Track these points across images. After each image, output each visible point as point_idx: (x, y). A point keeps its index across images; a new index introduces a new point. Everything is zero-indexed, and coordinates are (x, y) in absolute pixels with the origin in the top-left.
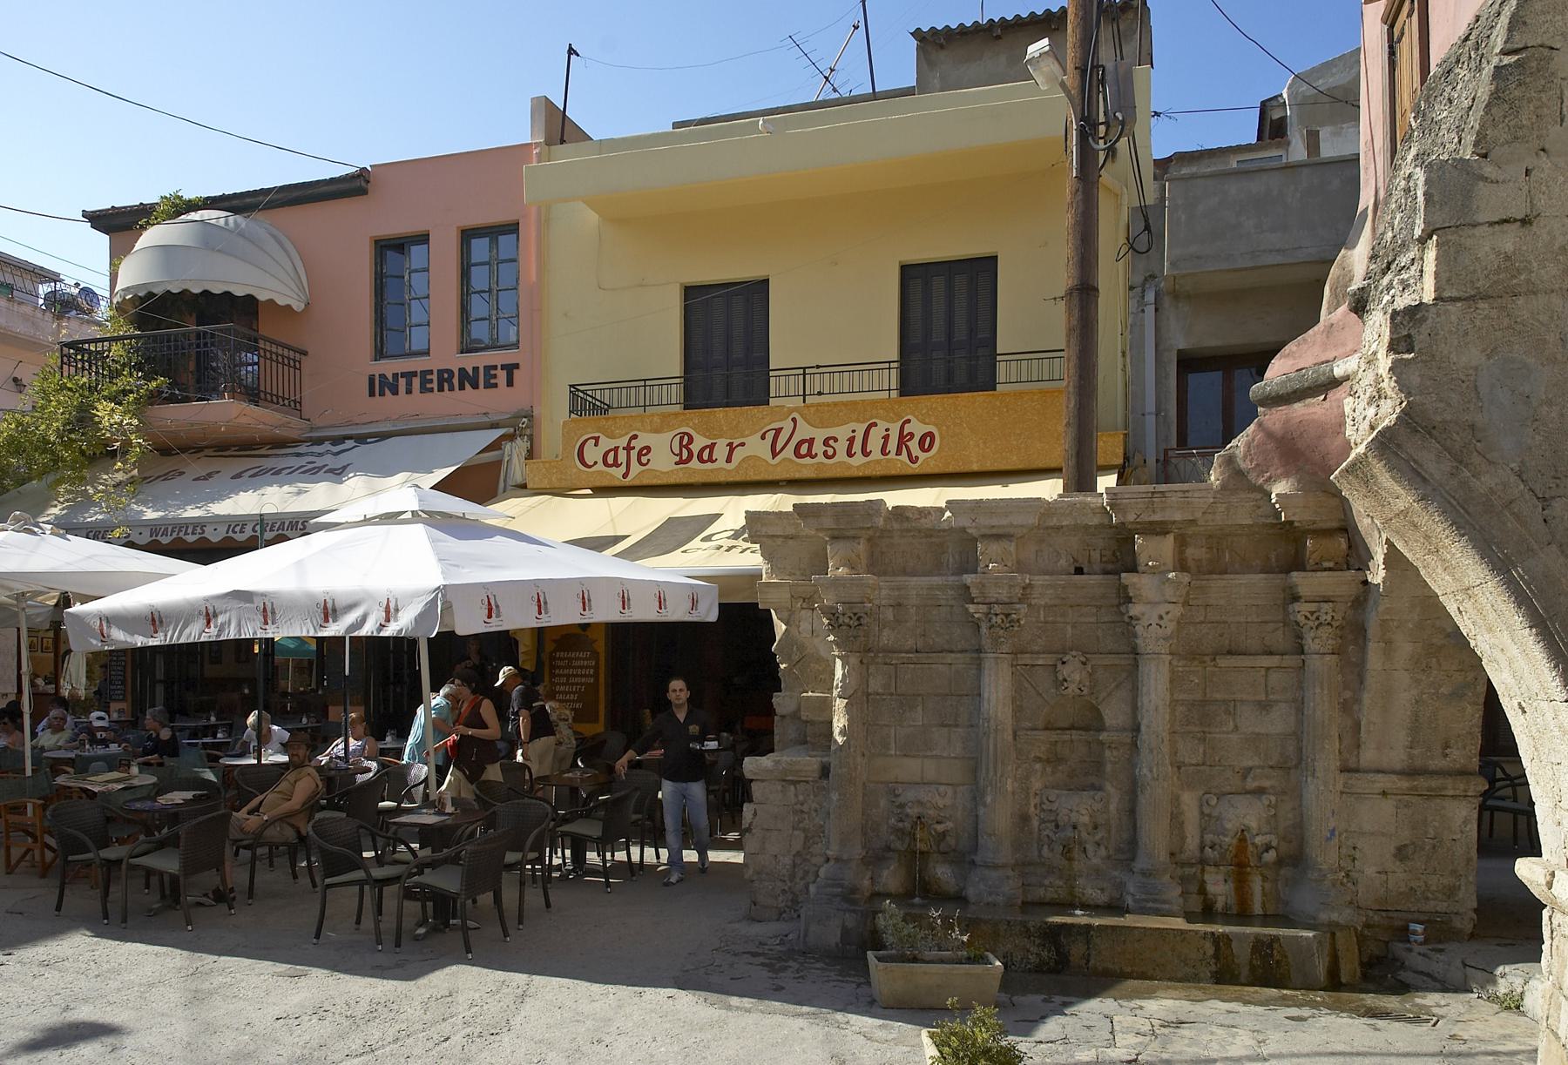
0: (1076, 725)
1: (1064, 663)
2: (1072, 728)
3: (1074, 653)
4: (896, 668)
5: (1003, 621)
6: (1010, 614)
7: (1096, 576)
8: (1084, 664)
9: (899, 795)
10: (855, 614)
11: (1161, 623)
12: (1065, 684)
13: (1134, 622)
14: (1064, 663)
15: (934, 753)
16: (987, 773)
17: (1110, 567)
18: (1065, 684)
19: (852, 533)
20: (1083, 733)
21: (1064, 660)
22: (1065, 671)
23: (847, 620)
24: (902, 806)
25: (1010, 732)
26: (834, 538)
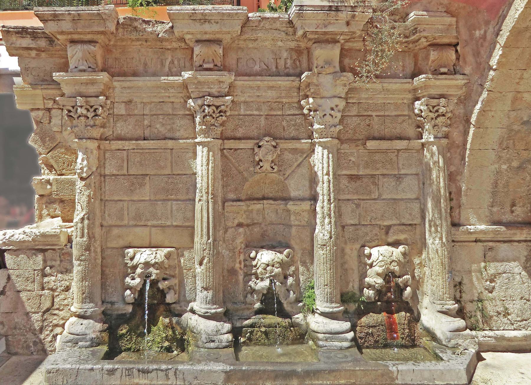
0: (266, 196)
1: (260, 147)
2: (264, 198)
3: (267, 139)
4: (128, 153)
5: (214, 112)
6: (220, 106)
8: (275, 147)
12: (261, 164)
14: (260, 147)
15: (160, 222)
19: (89, 37)
21: (260, 144)
22: (260, 154)
23: (84, 112)
25: (220, 203)
26: (73, 42)
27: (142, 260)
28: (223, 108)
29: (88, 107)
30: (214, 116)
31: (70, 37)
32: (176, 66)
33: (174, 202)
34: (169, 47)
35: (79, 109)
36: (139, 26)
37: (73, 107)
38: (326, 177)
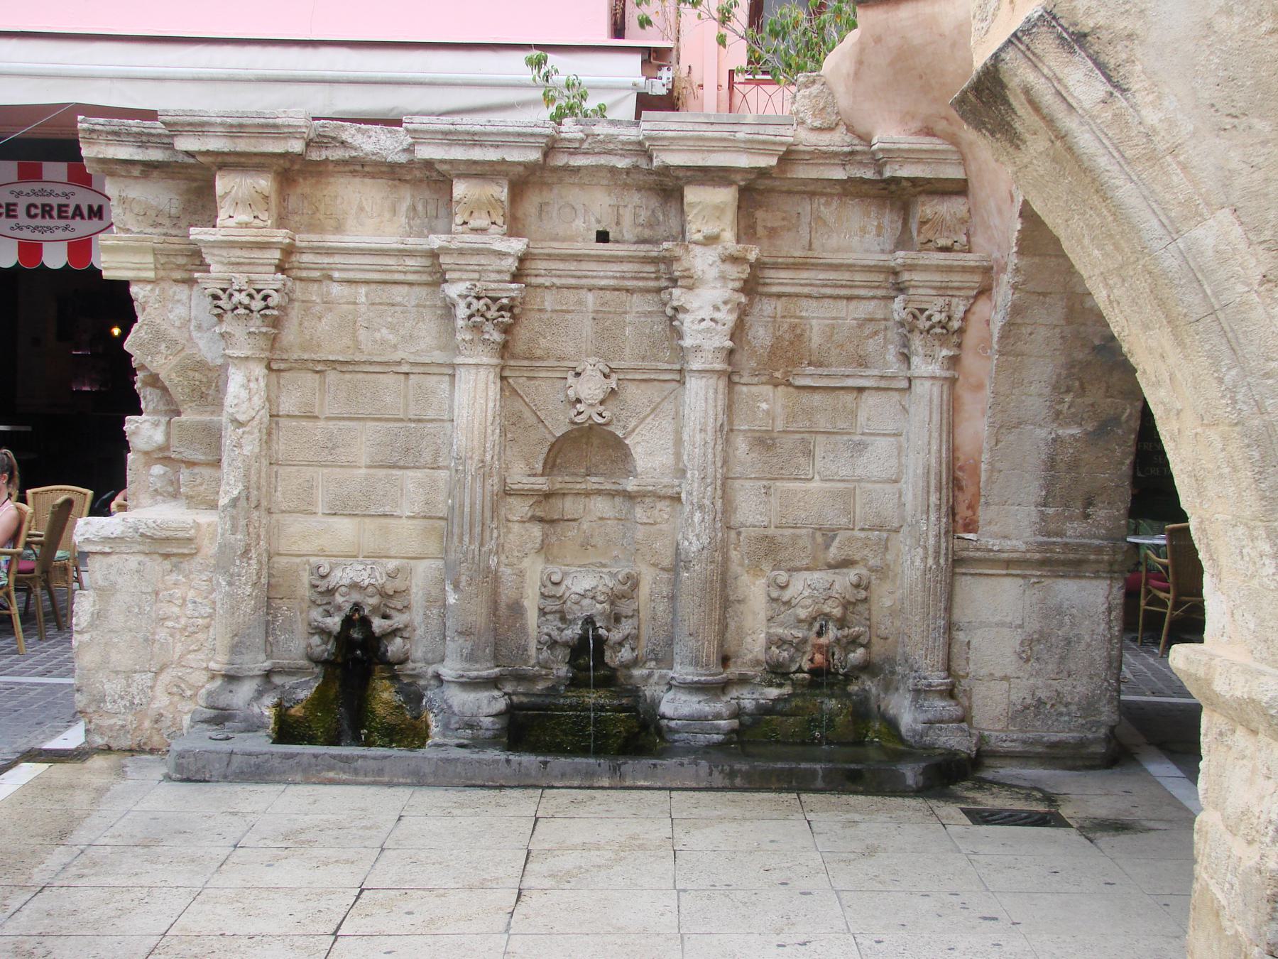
5: (489, 308)
7: (625, 247)
8: (606, 376)
9: (323, 577)
10: (259, 291)
11: (717, 315)
13: (680, 316)
14: (578, 374)
16: (461, 540)
17: (647, 233)
18: (578, 406)
20: (601, 479)
21: (578, 370)
23: (246, 301)
24: (331, 592)
27: (346, 581)
28: (505, 301)
29: (254, 292)
30: (489, 315)
31: (220, 159)
32: (421, 215)
33: (410, 473)
34: (408, 177)
35: (236, 294)
36: (350, 140)
37: (224, 290)
38: (698, 437)
